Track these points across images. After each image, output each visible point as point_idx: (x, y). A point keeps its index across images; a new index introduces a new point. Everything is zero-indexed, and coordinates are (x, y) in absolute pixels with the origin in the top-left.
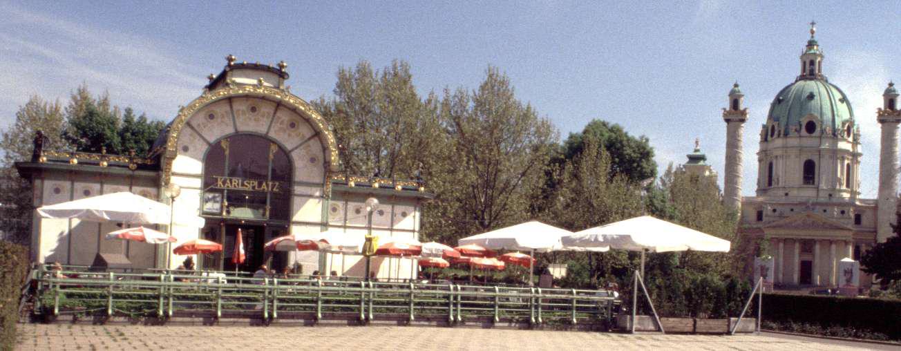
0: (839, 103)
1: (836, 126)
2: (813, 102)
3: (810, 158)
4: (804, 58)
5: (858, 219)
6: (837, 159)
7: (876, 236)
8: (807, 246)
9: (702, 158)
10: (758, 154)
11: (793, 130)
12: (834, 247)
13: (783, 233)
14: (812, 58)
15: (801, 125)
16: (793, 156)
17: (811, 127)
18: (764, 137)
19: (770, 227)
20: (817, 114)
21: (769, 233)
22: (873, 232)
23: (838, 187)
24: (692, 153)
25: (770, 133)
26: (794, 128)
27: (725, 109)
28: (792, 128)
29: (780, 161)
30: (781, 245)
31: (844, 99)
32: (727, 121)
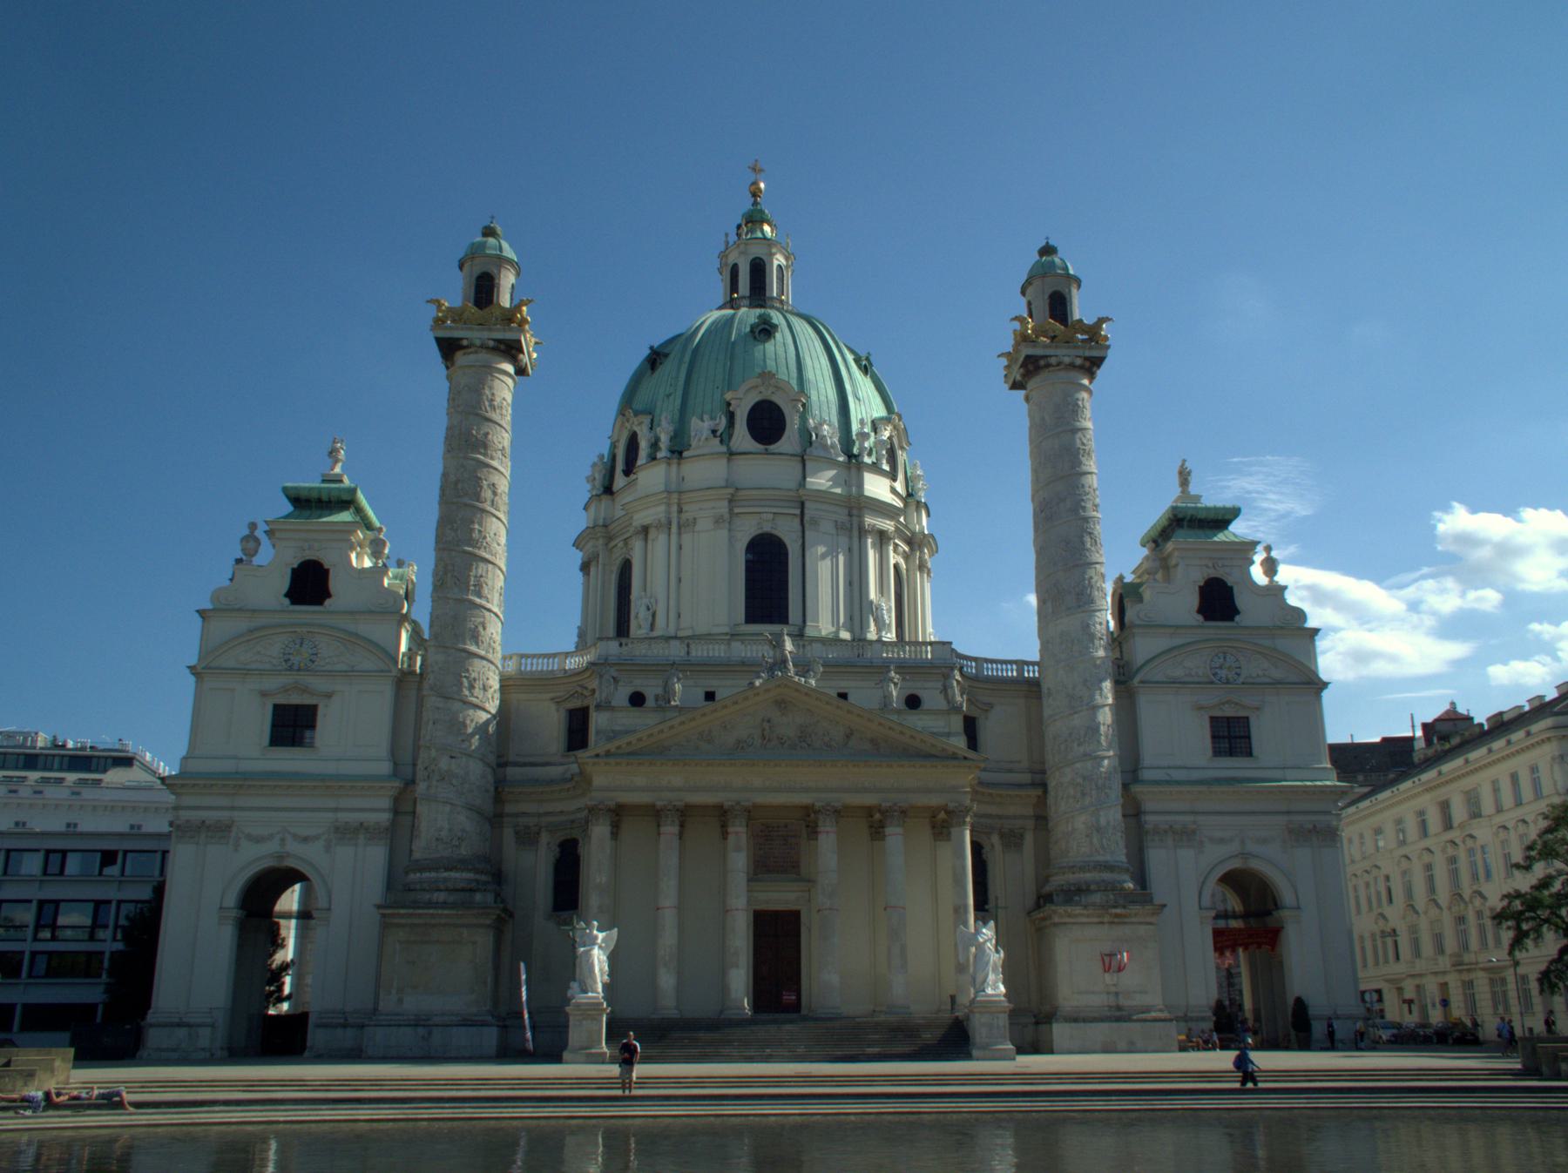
1: (855, 427)
2: (769, 346)
3: (767, 528)
4: (731, 260)
6: (862, 532)
7: (1042, 801)
8: (780, 842)
9: (346, 502)
10: (577, 544)
11: (706, 433)
14: (757, 251)
15: (731, 417)
16: (704, 524)
17: (767, 423)
18: (598, 483)
19: (608, 754)
20: (788, 375)
22: (1033, 785)
23: (872, 635)
24: (310, 482)
25: (620, 466)
26: (707, 425)
28: (700, 427)
29: (659, 542)
30: (670, 829)
32: (449, 348)
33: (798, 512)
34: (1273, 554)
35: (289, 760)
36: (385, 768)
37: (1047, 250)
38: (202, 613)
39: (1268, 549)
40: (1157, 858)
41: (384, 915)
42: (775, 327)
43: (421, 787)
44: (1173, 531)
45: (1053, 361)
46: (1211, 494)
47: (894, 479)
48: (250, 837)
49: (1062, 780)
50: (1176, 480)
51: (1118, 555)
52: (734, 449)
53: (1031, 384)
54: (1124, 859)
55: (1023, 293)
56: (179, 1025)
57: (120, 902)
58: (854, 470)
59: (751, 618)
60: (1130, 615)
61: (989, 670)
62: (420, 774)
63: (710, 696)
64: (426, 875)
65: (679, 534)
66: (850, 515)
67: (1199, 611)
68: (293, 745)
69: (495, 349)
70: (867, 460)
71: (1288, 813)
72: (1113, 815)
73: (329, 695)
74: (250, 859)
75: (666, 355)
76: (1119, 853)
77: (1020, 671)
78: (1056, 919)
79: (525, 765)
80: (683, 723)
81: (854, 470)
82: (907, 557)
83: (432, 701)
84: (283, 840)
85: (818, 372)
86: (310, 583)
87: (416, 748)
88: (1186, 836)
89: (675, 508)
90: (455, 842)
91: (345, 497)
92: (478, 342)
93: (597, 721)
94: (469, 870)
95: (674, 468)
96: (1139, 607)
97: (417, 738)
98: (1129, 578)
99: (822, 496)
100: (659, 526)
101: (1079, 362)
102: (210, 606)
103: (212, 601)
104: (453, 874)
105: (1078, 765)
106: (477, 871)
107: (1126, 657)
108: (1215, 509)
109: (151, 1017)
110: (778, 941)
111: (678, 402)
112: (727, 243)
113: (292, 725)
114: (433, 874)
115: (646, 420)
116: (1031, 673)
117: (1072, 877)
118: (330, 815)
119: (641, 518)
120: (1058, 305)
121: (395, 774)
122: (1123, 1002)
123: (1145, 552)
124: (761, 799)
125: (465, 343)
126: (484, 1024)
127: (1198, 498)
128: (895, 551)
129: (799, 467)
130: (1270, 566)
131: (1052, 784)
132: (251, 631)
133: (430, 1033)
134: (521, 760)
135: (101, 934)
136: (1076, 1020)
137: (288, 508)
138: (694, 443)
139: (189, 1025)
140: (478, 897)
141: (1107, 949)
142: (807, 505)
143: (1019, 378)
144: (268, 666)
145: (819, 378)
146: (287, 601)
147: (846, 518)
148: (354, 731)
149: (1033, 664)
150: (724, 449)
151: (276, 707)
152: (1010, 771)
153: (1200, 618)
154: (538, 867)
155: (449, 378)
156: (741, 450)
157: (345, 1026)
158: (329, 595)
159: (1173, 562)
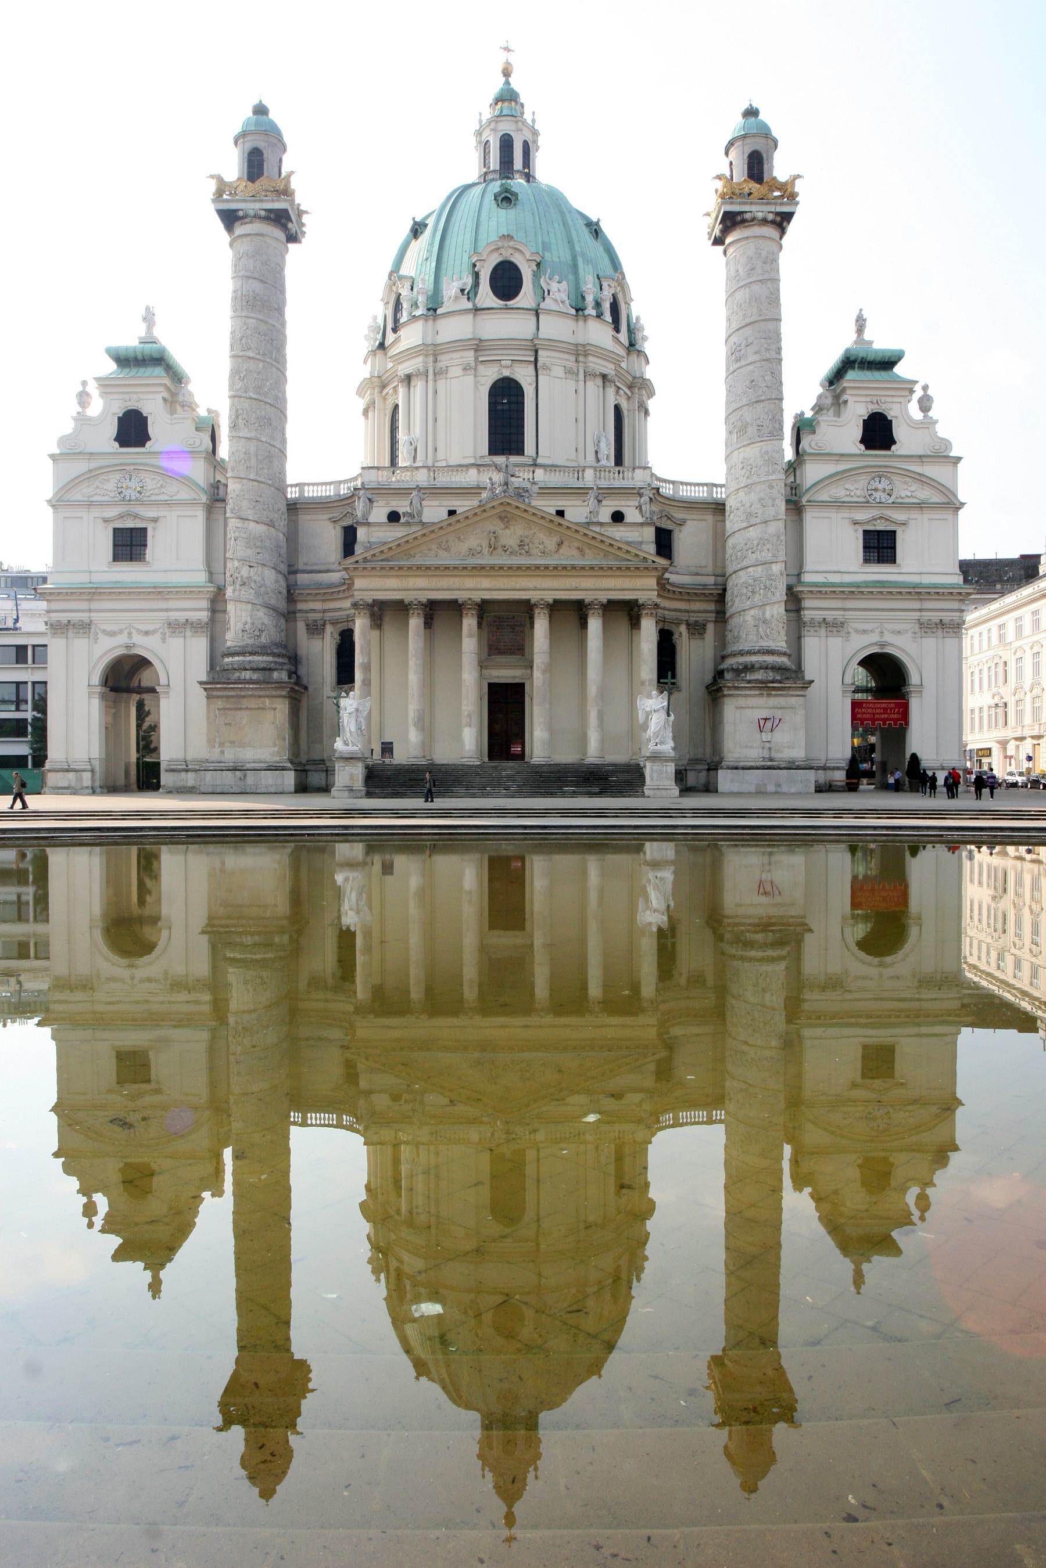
0: (586, 231)
3: (506, 373)
4: (484, 138)
5: (664, 542)
12: (595, 625)
13: (419, 588)
14: (506, 127)
15: (477, 275)
16: (456, 371)
17: (506, 281)
21: (374, 587)
25: (390, 325)
27: (220, 179)
28: (450, 290)
29: (418, 385)
30: (415, 623)
31: (595, 230)
32: (230, 218)
33: (532, 359)
34: (929, 392)
35: (129, 573)
36: (201, 578)
37: (751, 113)
38: (52, 457)
39: (925, 388)
40: (812, 645)
41: (205, 689)
42: (516, 195)
43: (229, 592)
44: (846, 372)
45: (748, 216)
46: (881, 341)
47: (617, 330)
48: (105, 632)
49: (737, 584)
50: (854, 328)
51: (801, 391)
52: (479, 306)
53: (728, 241)
54: (784, 644)
55: (727, 154)
56: (67, 771)
57: (34, 683)
58: (581, 323)
59: (494, 450)
60: (805, 444)
61: (685, 492)
62: (229, 579)
63: (452, 513)
64: (236, 658)
65: (435, 381)
66: (577, 361)
67: (862, 442)
68: (131, 560)
69: (266, 219)
70: (591, 311)
71: (920, 610)
72: (777, 611)
73: (155, 520)
74: (105, 649)
75: (426, 225)
76: (780, 643)
77: (710, 492)
78: (726, 692)
79: (311, 572)
80: (424, 535)
81: (581, 323)
82: (629, 398)
83: (233, 523)
84: (130, 634)
85: (552, 235)
86: (132, 430)
87: (225, 559)
88: (834, 627)
89: (431, 359)
90: (257, 633)
91: (156, 355)
92: (252, 213)
93: (361, 533)
94: (268, 655)
95: (430, 322)
96: (811, 437)
97: (225, 553)
98: (809, 414)
99: (554, 345)
100: (418, 374)
101: (771, 217)
102: (58, 451)
103: (59, 446)
104: (256, 658)
105: (751, 569)
106: (274, 655)
107: (798, 482)
108: (884, 351)
109: (48, 765)
110: (506, 708)
111: (434, 264)
112: (480, 121)
113: (130, 544)
114: (241, 658)
115: (408, 285)
116: (719, 494)
117: (742, 659)
118: (165, 614)
119: (404, 369)
120: (756, 165)
121: (211, 581)
122: (774, 755)
123: (820, 390)
124: (487, 596)
125: (241, 213)
126: (284, 769)
127: (871, 343)
128: (617, 393)
129: (534, 319)
130: (925, 404)
131: (730, 585)
132: (90, 471)
133: (245, 776)
134: (308, 568)
135: (23, 707)
136: (736, 768)
137: (113, 366)
138: (445, 299)
139: (76, 771)
140: (275, 675)
141: (765, 714)
142: (540, 353)
143: (718, 234)
144: (106, 498)
145: (553, 241)
146: (117, 444)
147: (571, 364)
148: (178, 549)
149: (722, 486)
150: (470, 305)
151: (115, 529)
152: (697, 574)
153: (862, 447)
154: (321, 653)
155: (231, 245)
156: (485, 306)
157: (187, 771)
158: (148, 438)
159: (845, 397)
